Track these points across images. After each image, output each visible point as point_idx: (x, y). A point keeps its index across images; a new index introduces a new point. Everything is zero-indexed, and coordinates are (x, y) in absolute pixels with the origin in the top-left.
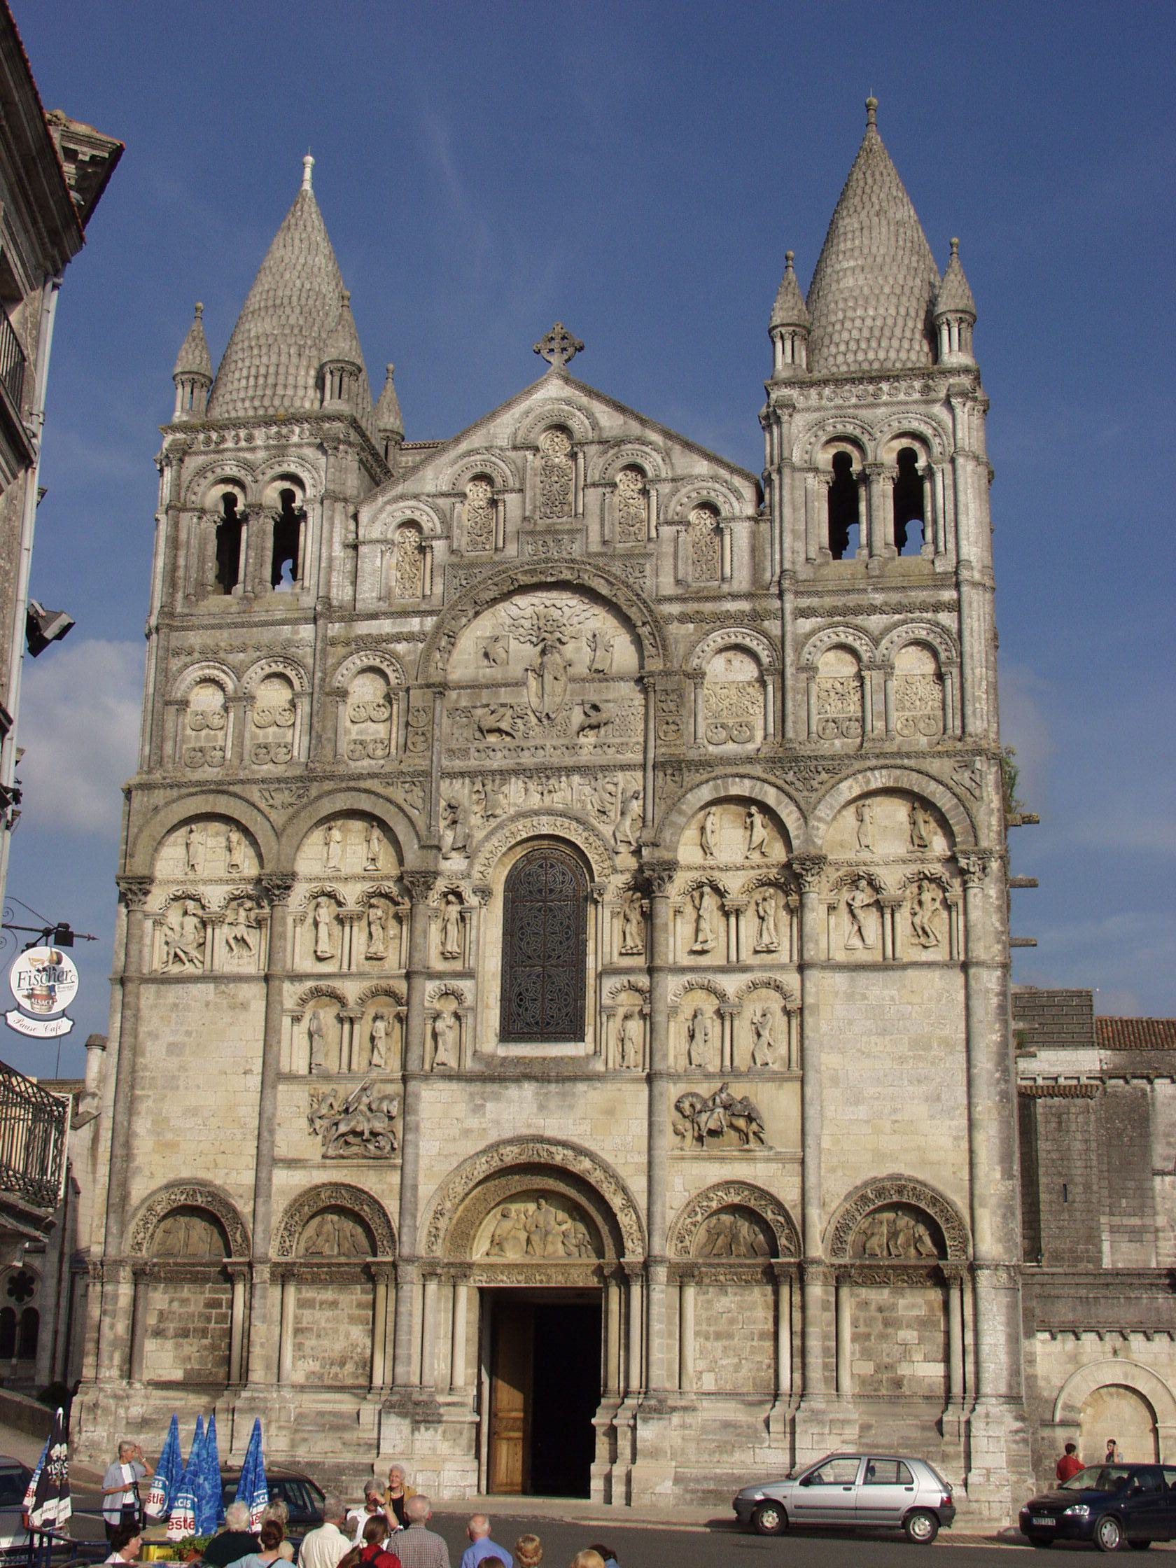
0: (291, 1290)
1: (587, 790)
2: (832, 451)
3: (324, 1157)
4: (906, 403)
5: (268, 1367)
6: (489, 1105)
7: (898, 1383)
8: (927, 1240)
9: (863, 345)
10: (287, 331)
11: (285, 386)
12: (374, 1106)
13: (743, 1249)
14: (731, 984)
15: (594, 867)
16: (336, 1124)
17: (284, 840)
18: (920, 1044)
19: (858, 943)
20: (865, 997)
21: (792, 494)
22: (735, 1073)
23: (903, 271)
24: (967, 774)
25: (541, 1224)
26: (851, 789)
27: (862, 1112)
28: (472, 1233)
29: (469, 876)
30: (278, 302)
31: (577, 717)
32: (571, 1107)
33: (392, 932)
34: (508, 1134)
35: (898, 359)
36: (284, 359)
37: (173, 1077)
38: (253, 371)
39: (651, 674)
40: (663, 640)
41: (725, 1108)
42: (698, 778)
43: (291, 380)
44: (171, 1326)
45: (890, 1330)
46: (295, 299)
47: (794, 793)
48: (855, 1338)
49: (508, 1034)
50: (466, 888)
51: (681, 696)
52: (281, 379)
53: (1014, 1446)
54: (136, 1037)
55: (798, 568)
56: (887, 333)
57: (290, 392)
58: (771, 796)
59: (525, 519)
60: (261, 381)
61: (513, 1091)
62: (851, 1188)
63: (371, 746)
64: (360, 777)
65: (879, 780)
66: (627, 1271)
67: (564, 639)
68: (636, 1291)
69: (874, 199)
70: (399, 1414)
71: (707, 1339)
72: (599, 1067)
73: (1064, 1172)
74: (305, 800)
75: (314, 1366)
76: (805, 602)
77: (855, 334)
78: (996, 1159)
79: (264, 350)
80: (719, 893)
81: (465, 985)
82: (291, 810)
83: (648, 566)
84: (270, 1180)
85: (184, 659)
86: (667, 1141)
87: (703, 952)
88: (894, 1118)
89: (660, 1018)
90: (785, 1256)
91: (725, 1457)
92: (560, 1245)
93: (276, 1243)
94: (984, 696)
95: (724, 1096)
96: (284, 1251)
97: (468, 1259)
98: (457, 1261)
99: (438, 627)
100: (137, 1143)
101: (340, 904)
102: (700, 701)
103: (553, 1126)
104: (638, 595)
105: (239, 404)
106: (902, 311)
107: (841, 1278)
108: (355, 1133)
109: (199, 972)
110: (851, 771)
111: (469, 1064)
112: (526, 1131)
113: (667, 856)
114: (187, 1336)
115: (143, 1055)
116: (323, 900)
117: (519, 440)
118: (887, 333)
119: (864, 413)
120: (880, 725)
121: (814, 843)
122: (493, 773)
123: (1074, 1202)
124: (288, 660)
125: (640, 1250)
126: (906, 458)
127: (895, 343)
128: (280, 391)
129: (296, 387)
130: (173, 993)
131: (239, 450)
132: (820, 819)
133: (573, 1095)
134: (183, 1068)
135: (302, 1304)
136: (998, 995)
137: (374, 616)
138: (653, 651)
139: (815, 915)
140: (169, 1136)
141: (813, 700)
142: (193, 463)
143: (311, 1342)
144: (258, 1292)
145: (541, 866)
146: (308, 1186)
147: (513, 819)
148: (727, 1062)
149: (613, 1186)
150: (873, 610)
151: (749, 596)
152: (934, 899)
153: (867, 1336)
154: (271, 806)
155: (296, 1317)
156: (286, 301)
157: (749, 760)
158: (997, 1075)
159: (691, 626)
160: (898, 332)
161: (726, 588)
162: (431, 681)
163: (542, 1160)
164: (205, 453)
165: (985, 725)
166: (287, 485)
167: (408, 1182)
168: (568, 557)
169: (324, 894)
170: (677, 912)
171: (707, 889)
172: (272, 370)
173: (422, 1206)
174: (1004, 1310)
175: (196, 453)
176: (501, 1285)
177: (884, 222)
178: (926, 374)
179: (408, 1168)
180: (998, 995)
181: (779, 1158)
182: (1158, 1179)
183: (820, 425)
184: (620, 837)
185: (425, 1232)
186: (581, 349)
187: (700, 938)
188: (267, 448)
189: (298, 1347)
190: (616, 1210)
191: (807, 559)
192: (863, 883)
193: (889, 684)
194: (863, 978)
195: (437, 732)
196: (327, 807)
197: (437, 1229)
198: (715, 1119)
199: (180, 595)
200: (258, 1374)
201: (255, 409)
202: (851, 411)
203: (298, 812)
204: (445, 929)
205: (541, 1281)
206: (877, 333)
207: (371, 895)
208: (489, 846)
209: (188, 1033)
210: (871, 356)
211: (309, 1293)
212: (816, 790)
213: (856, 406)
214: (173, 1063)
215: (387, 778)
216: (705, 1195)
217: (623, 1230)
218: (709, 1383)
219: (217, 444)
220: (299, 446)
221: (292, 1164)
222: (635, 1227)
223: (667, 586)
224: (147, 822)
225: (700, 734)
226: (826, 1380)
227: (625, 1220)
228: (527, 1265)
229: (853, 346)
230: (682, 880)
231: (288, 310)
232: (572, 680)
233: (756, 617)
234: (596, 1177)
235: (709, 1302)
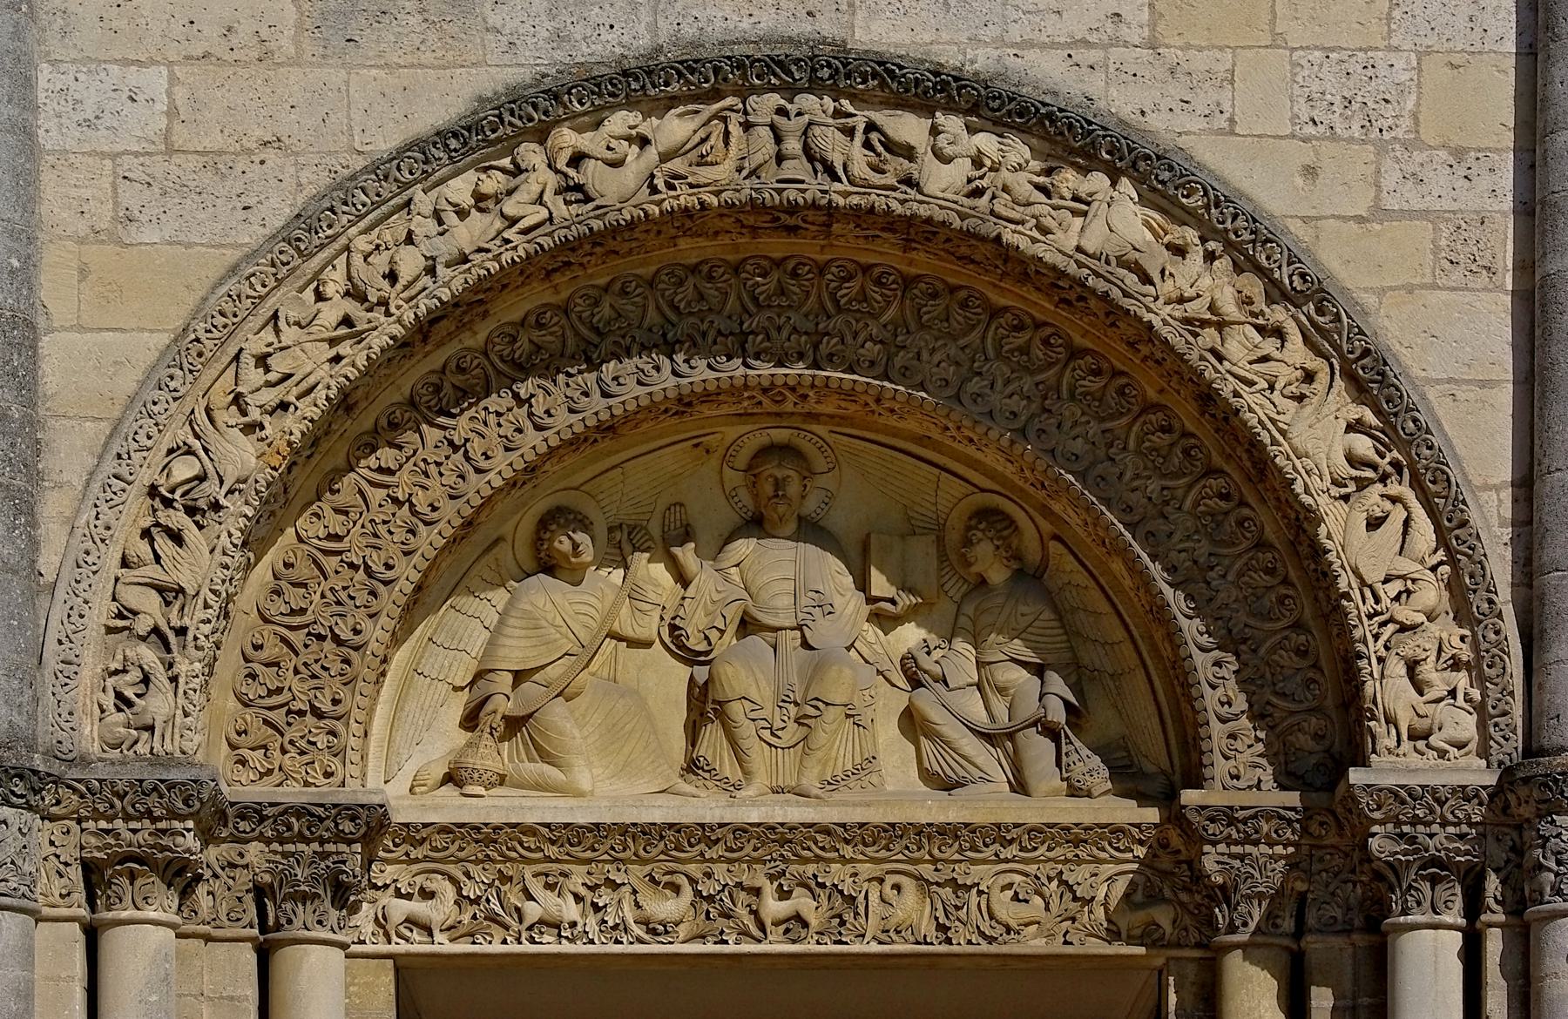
25: (779, 608)
28: (376, 634)
66: (1380, 844)
92: (888, 732)
97: (351, 794)
98: (293, 793)
125: (1467, 726)
149: (1297, 351)
163: (839, 194)
176: (549, 944)
185: (101, 612)
197: (169, 593)
217: (1359, 606)
222: (1431, 593)
228: (705, 834)
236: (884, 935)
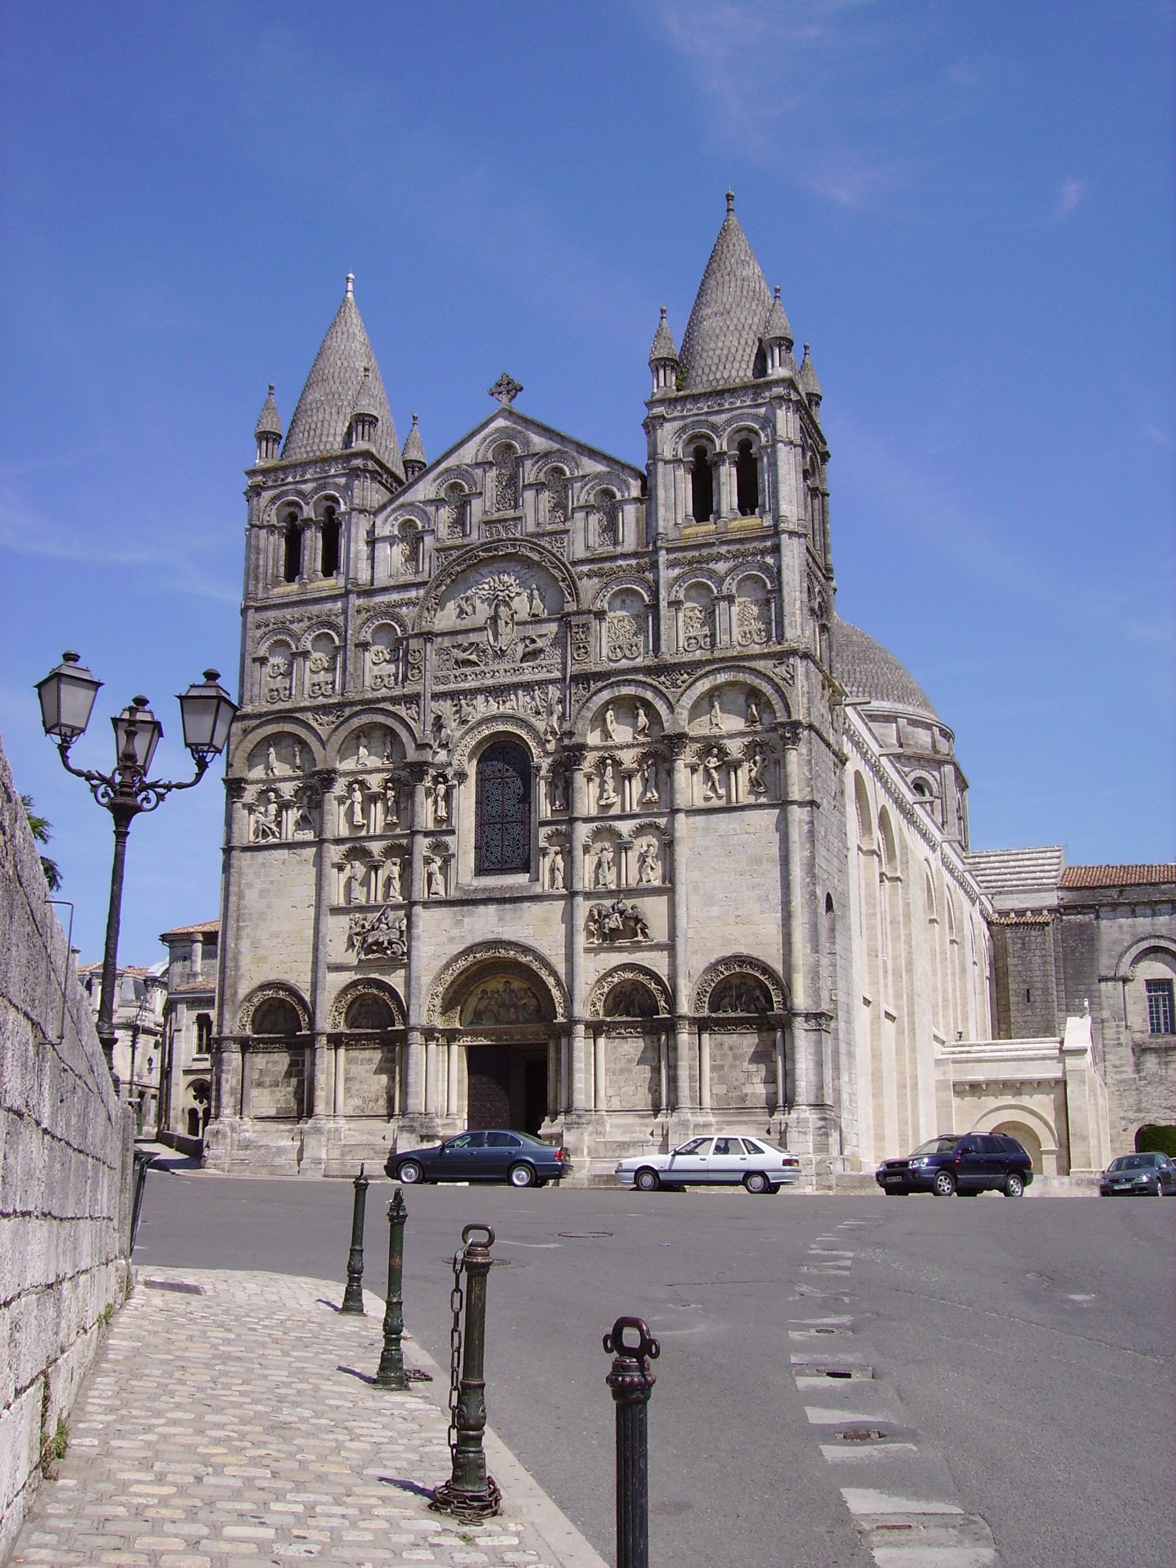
0: (342, 1051)
1: (528, 699)
2: (693, 446)
3: (360, 961)
4: (742, 408)
5: (327, 1103)
6: (465, 919)
7: (743, 1099)
8: (762, 998)
9: (714, 369)
10: (330, 397)
11: (328, 435)
12: (390, 924)
13: (637, 1011)
15: (533, 751)
16: (364, 941)
17: (328, 748)
18: (756, 860)
19: (713, 795)
20: (716, 830)
21: (664, 478)
22: (631, 892)
23: (745, 313)
24: (784, 668)
26: (704, 685)
27: (715, 911)
29: (450, 764)
30: (325, 378)
31: (520, 649)
32: (520, 918)
33: (402, 806)
34: (478, 939)
35: (738, 376)
36: (327, 417)
37: (263, 913)
38: (307, 428)
39: (569, 614)
40: (576, 589)
41: (622, 913)
42: (600, 684)
43: (332, 431)
44: (267, 1080)
45: (737, 1062)
46: (336, 374)
47: (665, 690)
48: (713, 1068)
49: (480, 871)
50: (450, 772)
51: (588, 629)
52: (325, 432)
53: (819, 1138)
54: (239, 887)
55: (669, 531)
56: (731, 359)
57: (331, 439)
58: (649, 695)
59: (486, 512)
60: (312, 433)
61: (481, 909)
62: (708, 965)
63: (386, 680)
64: (378, 700)
65: (722, 678)
67: (512, 595)
68: (564, 1041)
69: (728, 264)
70: (408, 1131)
71: (614, 1074)
72: (537, 889)
73: (1027, 980)
74: (341, 719)
75: (357, 1102)
76: (672, 556)
77: (709, 362)
78: (808, 939)
79: (315, 411)
80: (617, 763)
81: (448, 839)
82: (333, 726)
83: (566, 540)
84: (325, 978)
85: (263, 629)
86: (581, 940)
87: (608, 806)
88: (737, 914)
89: (578, 852)
90: (663, 1013)
91: (624, 1153)
93: (330, 1021)
94: (798, 612)
95: (620, 905)
96: (336, 1026)
98: (449, 1027)
99: (427, 593)
100: (240, 958)
101: (369, 789)
102: (603, 631)
103: (509, 933)
104: (559, 560)
105: (298, 450)
106: (743, 342)
107: (702, 1026)
108: (376, 943)
109: (276, 841)
110: (703, 672)
111: (454, 894)
112: (490, 936)
113: (580, 740)
114: (278, 1086)
115: (244, 899)
116: (356, 786)
117: (479, 460)
118: (731, 359)
119: (714, 419)
120: (726, 638)
121: (679, 724)
122: (465, 693)
123: (1035, 1002)
124: (331, 625)
126: (745, 447)
127: (736, 365)
128: (324, 439)
129: (335, 435)
130: (261, 856)
131: (296, 483)
132: (683, 707)
133: (521, 909)
134: (269, 906)
135: (349, 1061)
136: (808, 823)
137: (385, 590)
138: (570, 599)
139: (682, 774)
140: (261, 952)
141: (681, 624)
142: (267, 495)
143: (355, 1086)
144: (318, 1055)
145: (500, 753)
146: (350, 981)
147: (480, 723)
148: (624, 882)
150: (719, 558)
151: (635, 555)
152: (764, 760)
153: (723, 1066)
154: (321, 724)
155: (345, 1070)
156: (330, 377)
157: (635, 670)
158: (808, 880)
159: (596, 580)
160: (738, 358)
161: (619, 550)
162: (423, 630)
163: (501, 955)
164: (275, 487)
165: (799, 632)
166: (329, 503)
167: (413, 974)
168: (512, 536)
169: (356, 781)
170: (589, 780)
171: (609, 761)
172: (319, 425)
173: (424, 991)
174: (813, 1044)
175: (269, 488)
177: (733, 279)
178: (756, 387)
179: (414, 965)
180: (808, 823)
181: (659, 947)
182: (1103, 984)
183: (683, 429)
184: (549, 730)
185: (427, 1008)
186: (521, 389)
187: (605, 796)
188: (315, 480)
189: (347, 1090)
190: (551, 987)
191: (676, 524)
192: (715, 751)
193: (732, 608)
194: (714, 818)
195: (428, 665)
196: (356, 722)
197: (434, 1006)
198: (614, 922)
199: (261, 585)
200: (320, 1107)
201: (307, 452)
202: (703, 418)
203: (337, 728)
204: (436, 802)
205: (507, 1040)
206: (723, 360)
207: (387, 781)
208: (463, 742)
209: (272, 882)
210: (718, 376)
211: (355, 1054)
212: (680, 687)
213: (707, 413)
214: (263, 902)
215: (395, 700)
216: (610, 974)
218: (616, 1105)
219: (283, 480)
220: (334, 476)
221: (338, 968)
223: (580, 553)
224: (241, 741)
225: (604, 653)
226: (692, 1099)
227: (556, 993)
229: (707, 370)
230: (591, 757)
231: (331, 382)
232: (518, 624)
233: (641, 569)
234: (535, 966)
235: (615, 1048)
236: (517, 1040)
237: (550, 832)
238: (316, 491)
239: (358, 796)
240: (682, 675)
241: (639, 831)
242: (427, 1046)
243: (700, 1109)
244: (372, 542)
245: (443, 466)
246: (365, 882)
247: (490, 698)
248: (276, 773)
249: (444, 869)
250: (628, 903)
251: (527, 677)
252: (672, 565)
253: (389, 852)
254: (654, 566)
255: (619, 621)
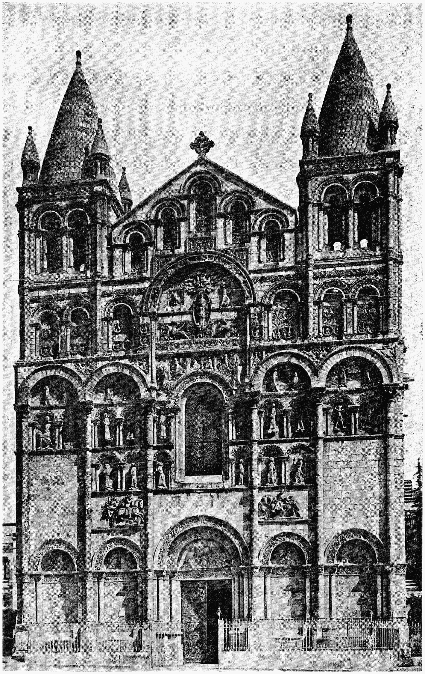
14: (285, 448)
72: (228, 485)
80: (279, 406)
99: (151, 285)
122: (179, 356)
154: (81, 372)
198: (278, 506)
216: (274, 538)
237: (236, 449)
238: (69, 207)
239: (107, 422)
240: (323, 351)
241: (294, 451)
242: (170, 581)
243: (331, 619)
244: (112, 247)
245: (158, 198)
246: (113, 476)
247: (195, 361)
248: (51, 403)
249: (167, 468)
250: (286, 495)
251: (220, 347)
252: (316, 277)
253: (130, 459)
254: (305, 277)
255: (280, 313)
